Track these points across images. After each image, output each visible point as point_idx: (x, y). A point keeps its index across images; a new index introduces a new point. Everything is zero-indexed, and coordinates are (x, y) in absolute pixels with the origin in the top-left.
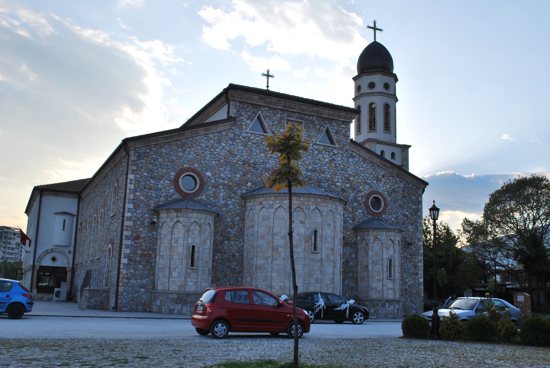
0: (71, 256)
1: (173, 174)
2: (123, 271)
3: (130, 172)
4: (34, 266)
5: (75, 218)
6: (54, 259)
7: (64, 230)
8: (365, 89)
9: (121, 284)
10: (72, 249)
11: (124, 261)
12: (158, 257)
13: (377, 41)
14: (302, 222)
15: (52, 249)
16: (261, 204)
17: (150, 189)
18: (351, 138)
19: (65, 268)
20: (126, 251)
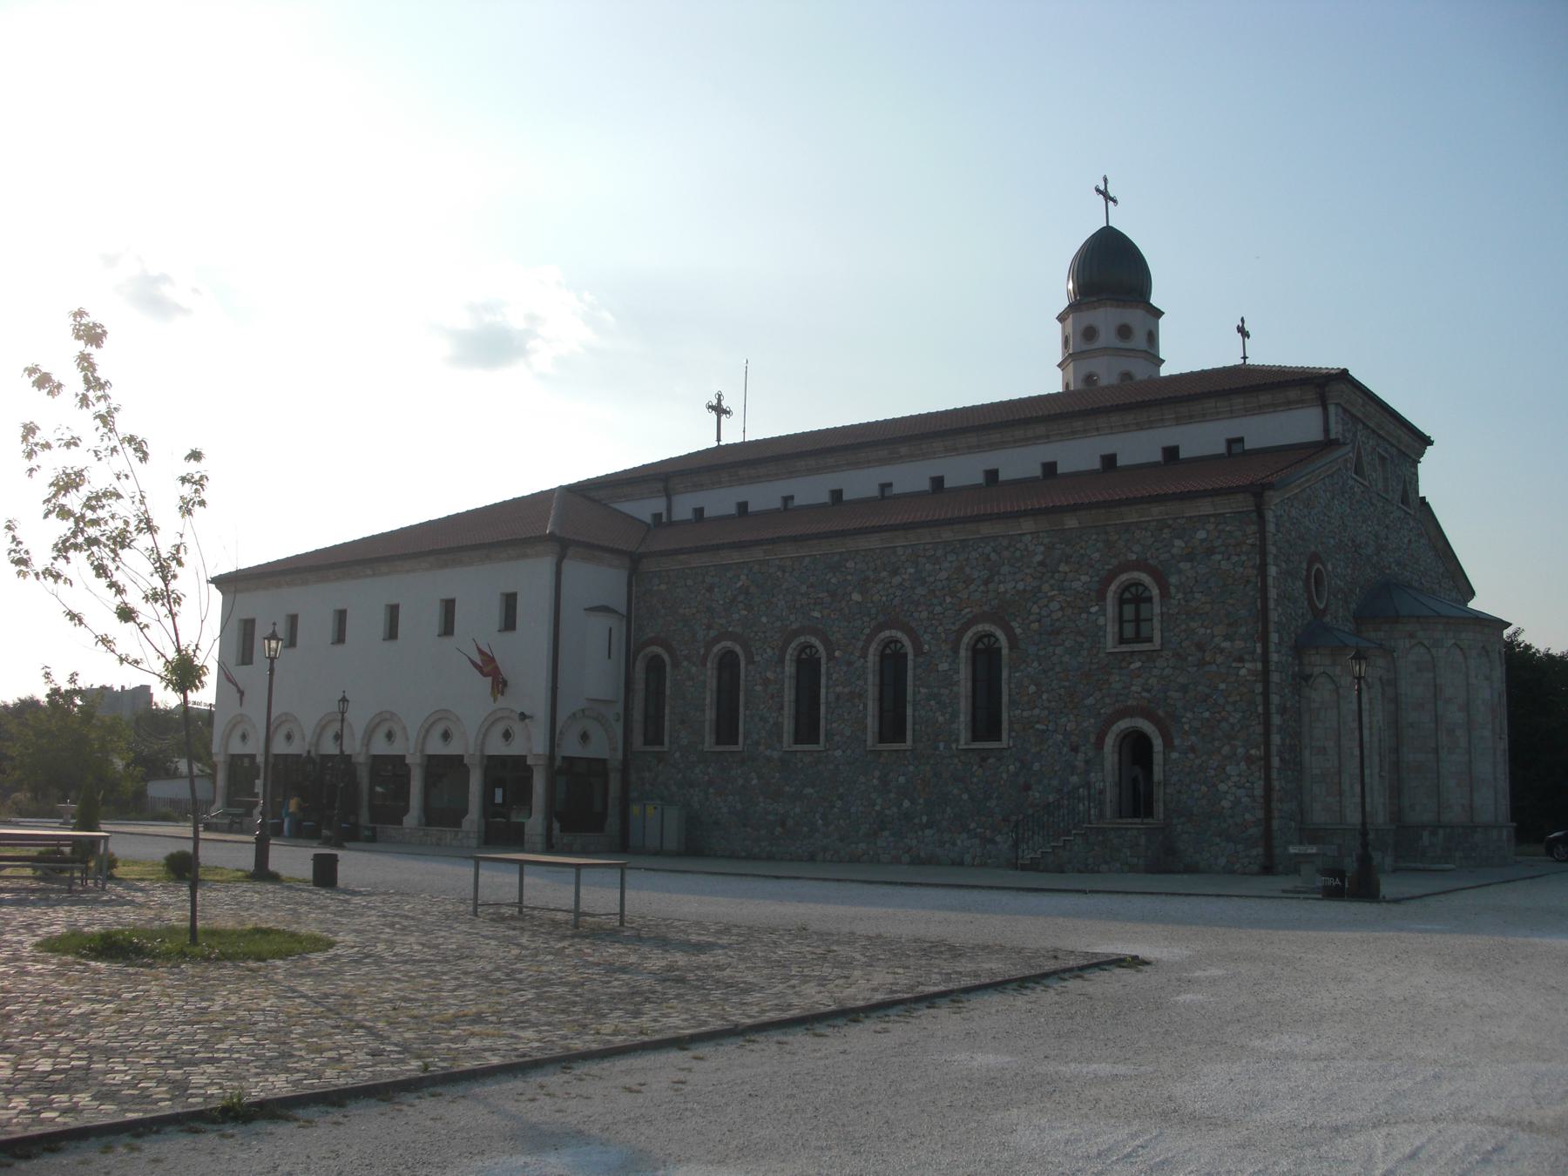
0: (619, 729)
1: (1304, 566)
2: (1276, 784)
3: (1270, 559)
4: (551, 757)
5: (624, 623)
6: (585, 737)
7: (609, 657)
8: (1107, 337)
9: (1276, 814)
10: (619, 708)
11: (1276, 762)
12: (1307, 753)
13: (1110, 225)
14: (1487, 678)
15: (583, 710)
16: (1411, 636)
17: (1288, 599)
18: (1421, 495)
19: (603, 762)
20: (1276, 739)
